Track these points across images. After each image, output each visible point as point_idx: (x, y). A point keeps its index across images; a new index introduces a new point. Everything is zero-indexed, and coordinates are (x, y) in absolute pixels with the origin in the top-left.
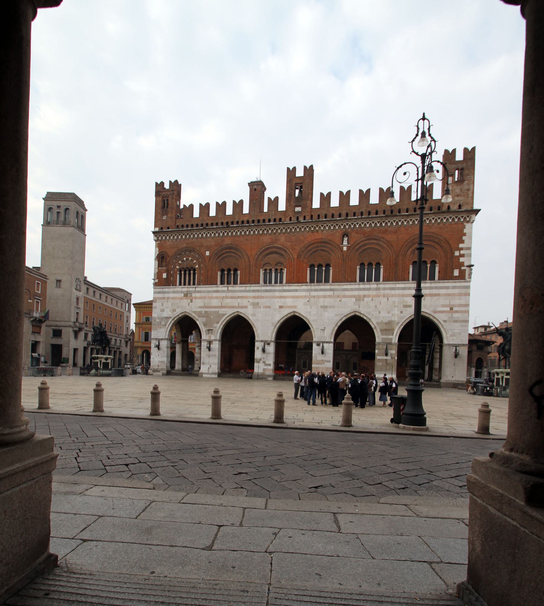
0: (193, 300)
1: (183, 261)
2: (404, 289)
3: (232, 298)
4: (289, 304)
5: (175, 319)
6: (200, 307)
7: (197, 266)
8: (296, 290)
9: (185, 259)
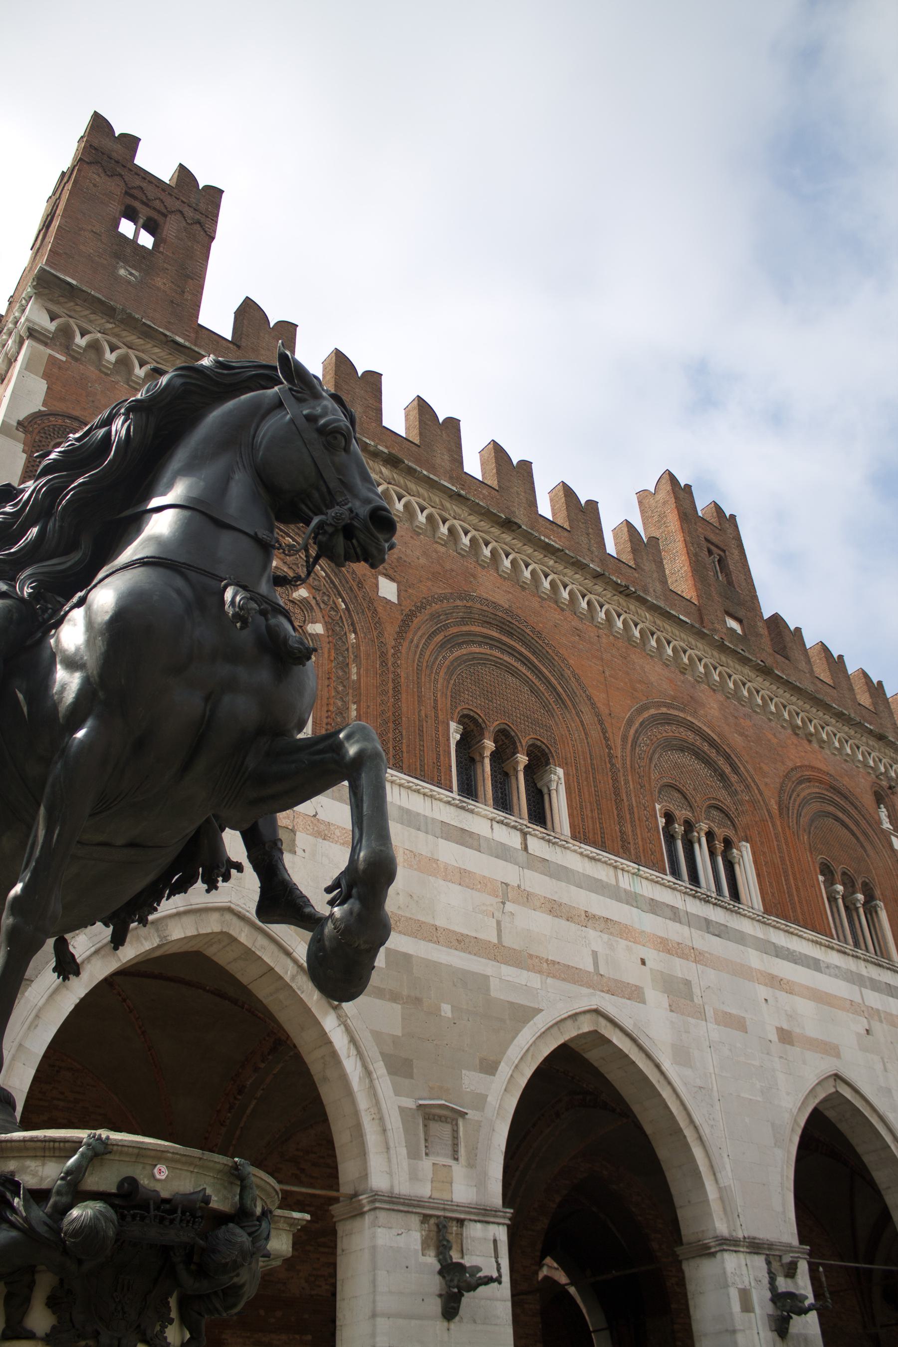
3: (554, 908)
4: (812, 1030)
8: (815, 965)
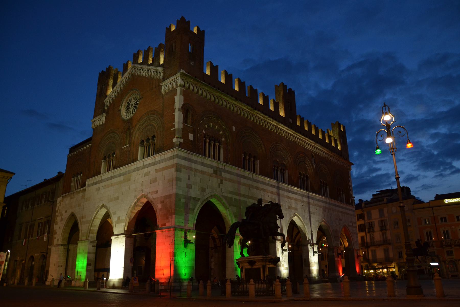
0: (224, 181)
1: (209, 126)
2: (338, 206)
5: (204, 203)
6: (231, 192)
7: (223, 139)
9: (211, 124)
